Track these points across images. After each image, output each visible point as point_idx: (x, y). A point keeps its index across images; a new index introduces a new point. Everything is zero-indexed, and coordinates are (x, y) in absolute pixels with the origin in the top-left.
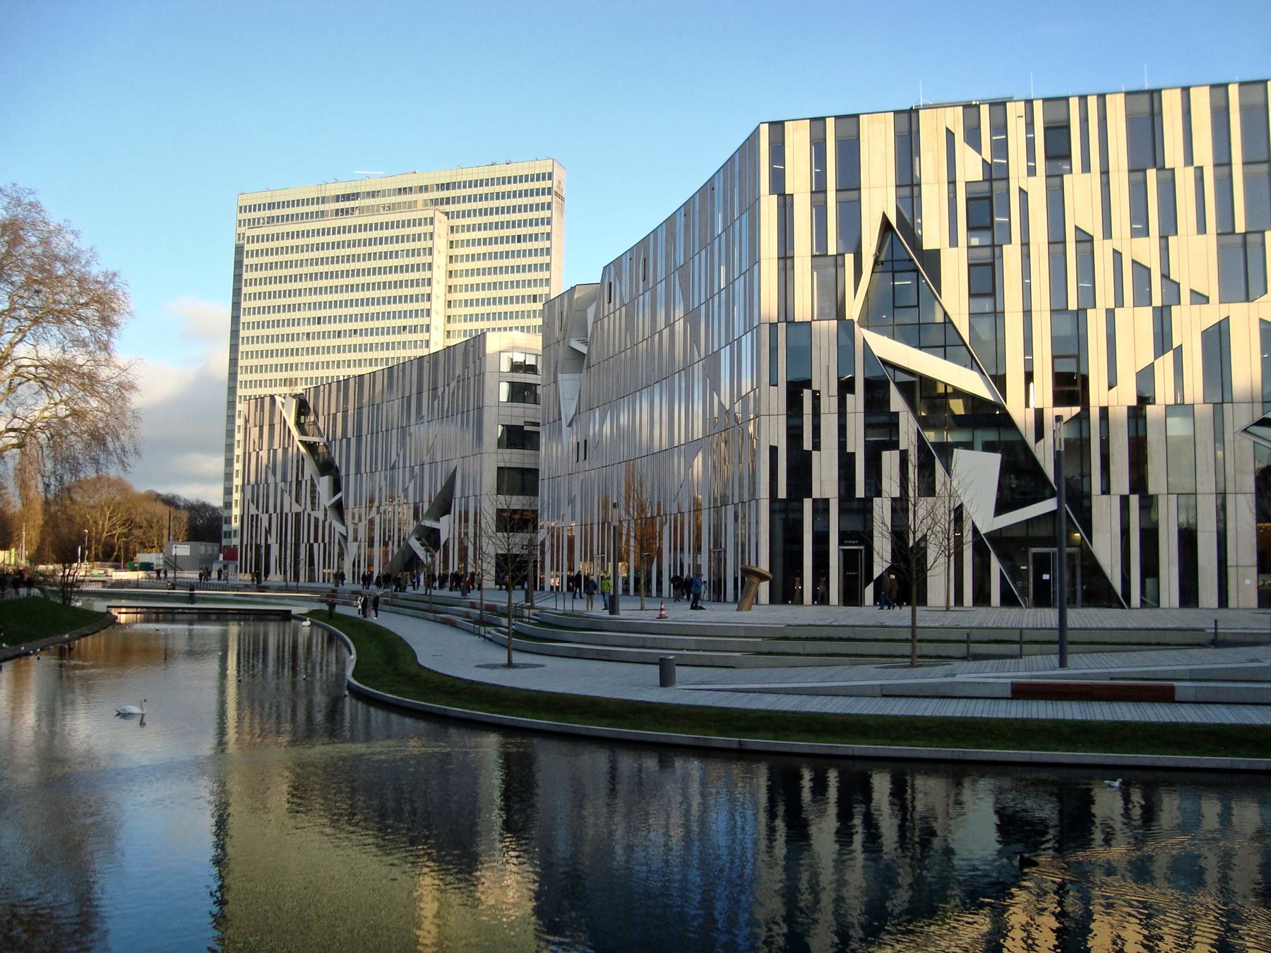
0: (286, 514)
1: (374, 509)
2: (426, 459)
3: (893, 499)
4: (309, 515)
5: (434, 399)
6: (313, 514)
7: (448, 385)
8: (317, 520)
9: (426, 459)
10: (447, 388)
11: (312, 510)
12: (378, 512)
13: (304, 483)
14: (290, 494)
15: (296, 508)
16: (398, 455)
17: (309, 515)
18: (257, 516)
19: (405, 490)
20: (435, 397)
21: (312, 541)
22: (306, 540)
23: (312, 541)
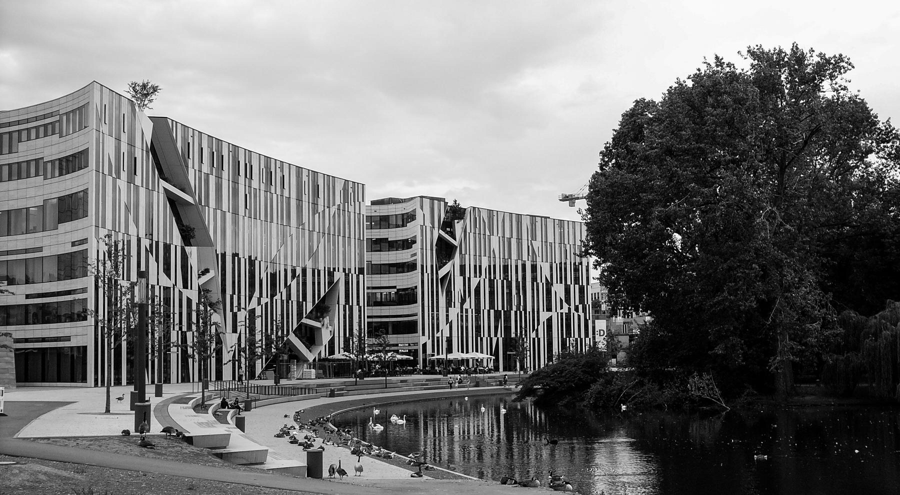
0: (153, 287)
1: (255, 300)
2: (309, 265)
3: (447, 337)
4: (180, 293)
5: (314, 214)
6: (186, 293)
7: (329, 207)
8: (189, 301)
9: (309, 265)
10: (327, 210)
11: (185, 286)
12: (259, 303)
13: (173, 248)
14: (157, 260)
15: (165, 282)
16: (279, 251)
17: (180, 293)
18: (116, 281)
19: (288, 288)
20: (315, 211)
21: (185, 329)
22: (177, 328)
23: (185, 329)
